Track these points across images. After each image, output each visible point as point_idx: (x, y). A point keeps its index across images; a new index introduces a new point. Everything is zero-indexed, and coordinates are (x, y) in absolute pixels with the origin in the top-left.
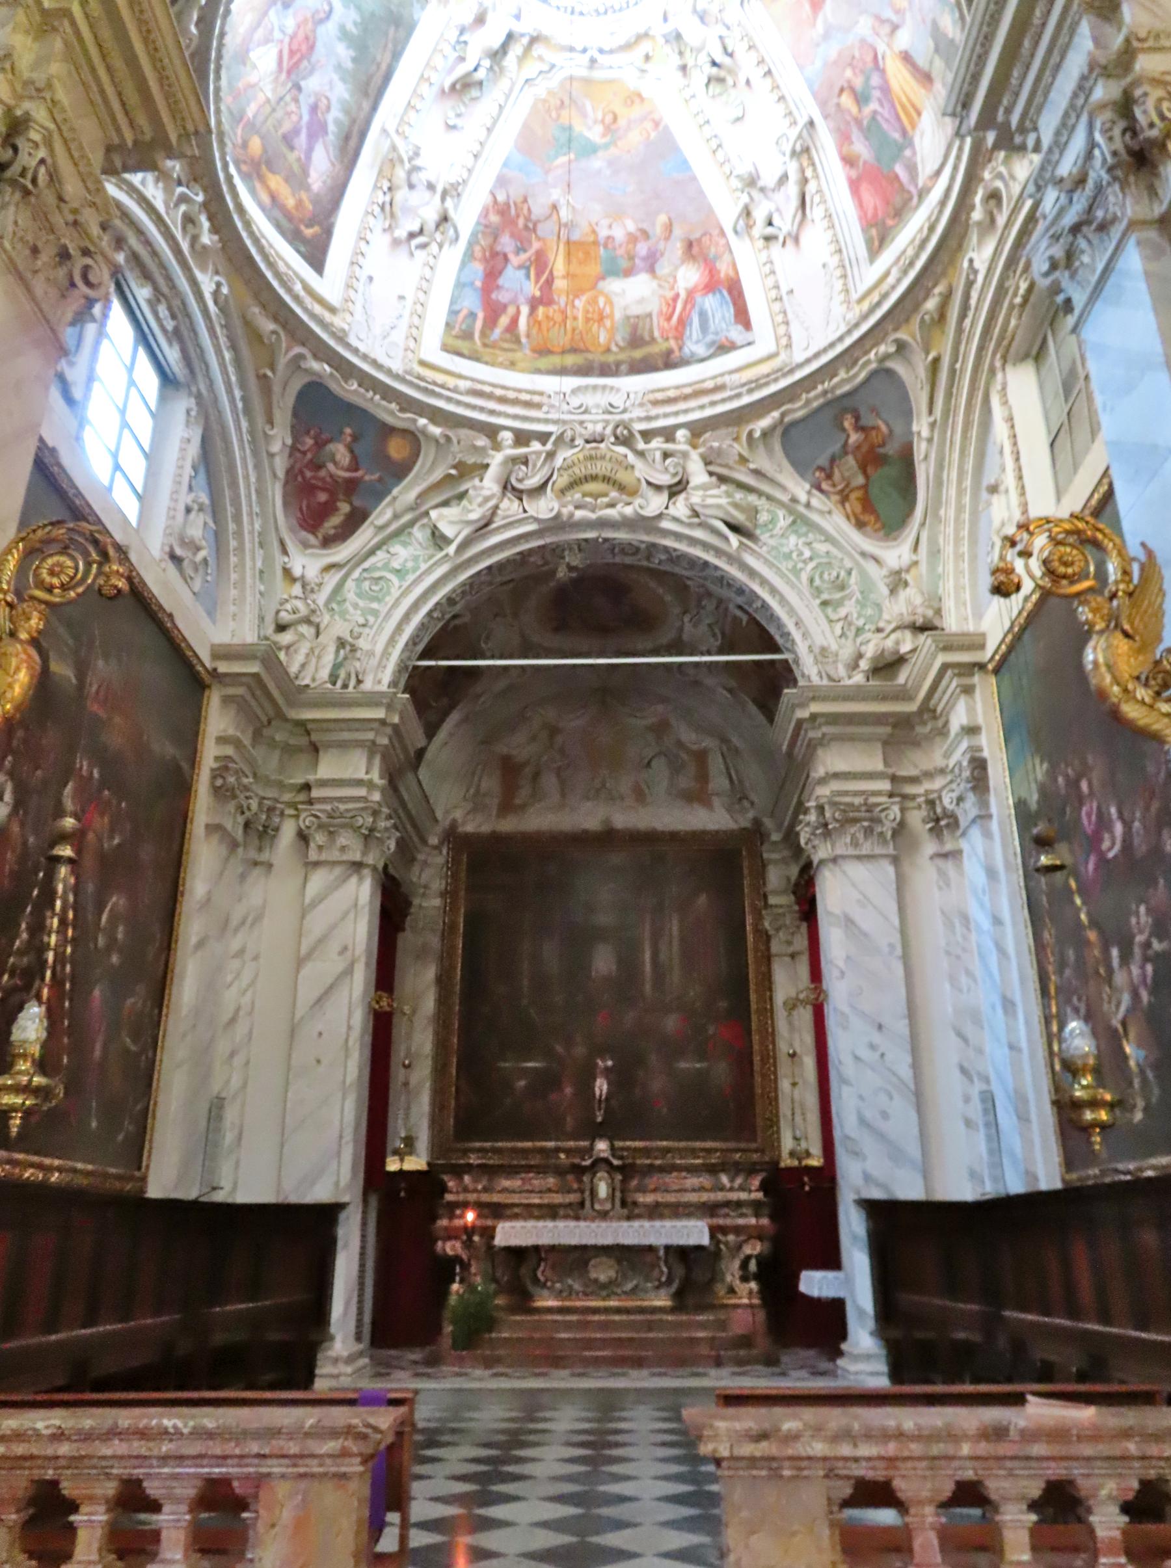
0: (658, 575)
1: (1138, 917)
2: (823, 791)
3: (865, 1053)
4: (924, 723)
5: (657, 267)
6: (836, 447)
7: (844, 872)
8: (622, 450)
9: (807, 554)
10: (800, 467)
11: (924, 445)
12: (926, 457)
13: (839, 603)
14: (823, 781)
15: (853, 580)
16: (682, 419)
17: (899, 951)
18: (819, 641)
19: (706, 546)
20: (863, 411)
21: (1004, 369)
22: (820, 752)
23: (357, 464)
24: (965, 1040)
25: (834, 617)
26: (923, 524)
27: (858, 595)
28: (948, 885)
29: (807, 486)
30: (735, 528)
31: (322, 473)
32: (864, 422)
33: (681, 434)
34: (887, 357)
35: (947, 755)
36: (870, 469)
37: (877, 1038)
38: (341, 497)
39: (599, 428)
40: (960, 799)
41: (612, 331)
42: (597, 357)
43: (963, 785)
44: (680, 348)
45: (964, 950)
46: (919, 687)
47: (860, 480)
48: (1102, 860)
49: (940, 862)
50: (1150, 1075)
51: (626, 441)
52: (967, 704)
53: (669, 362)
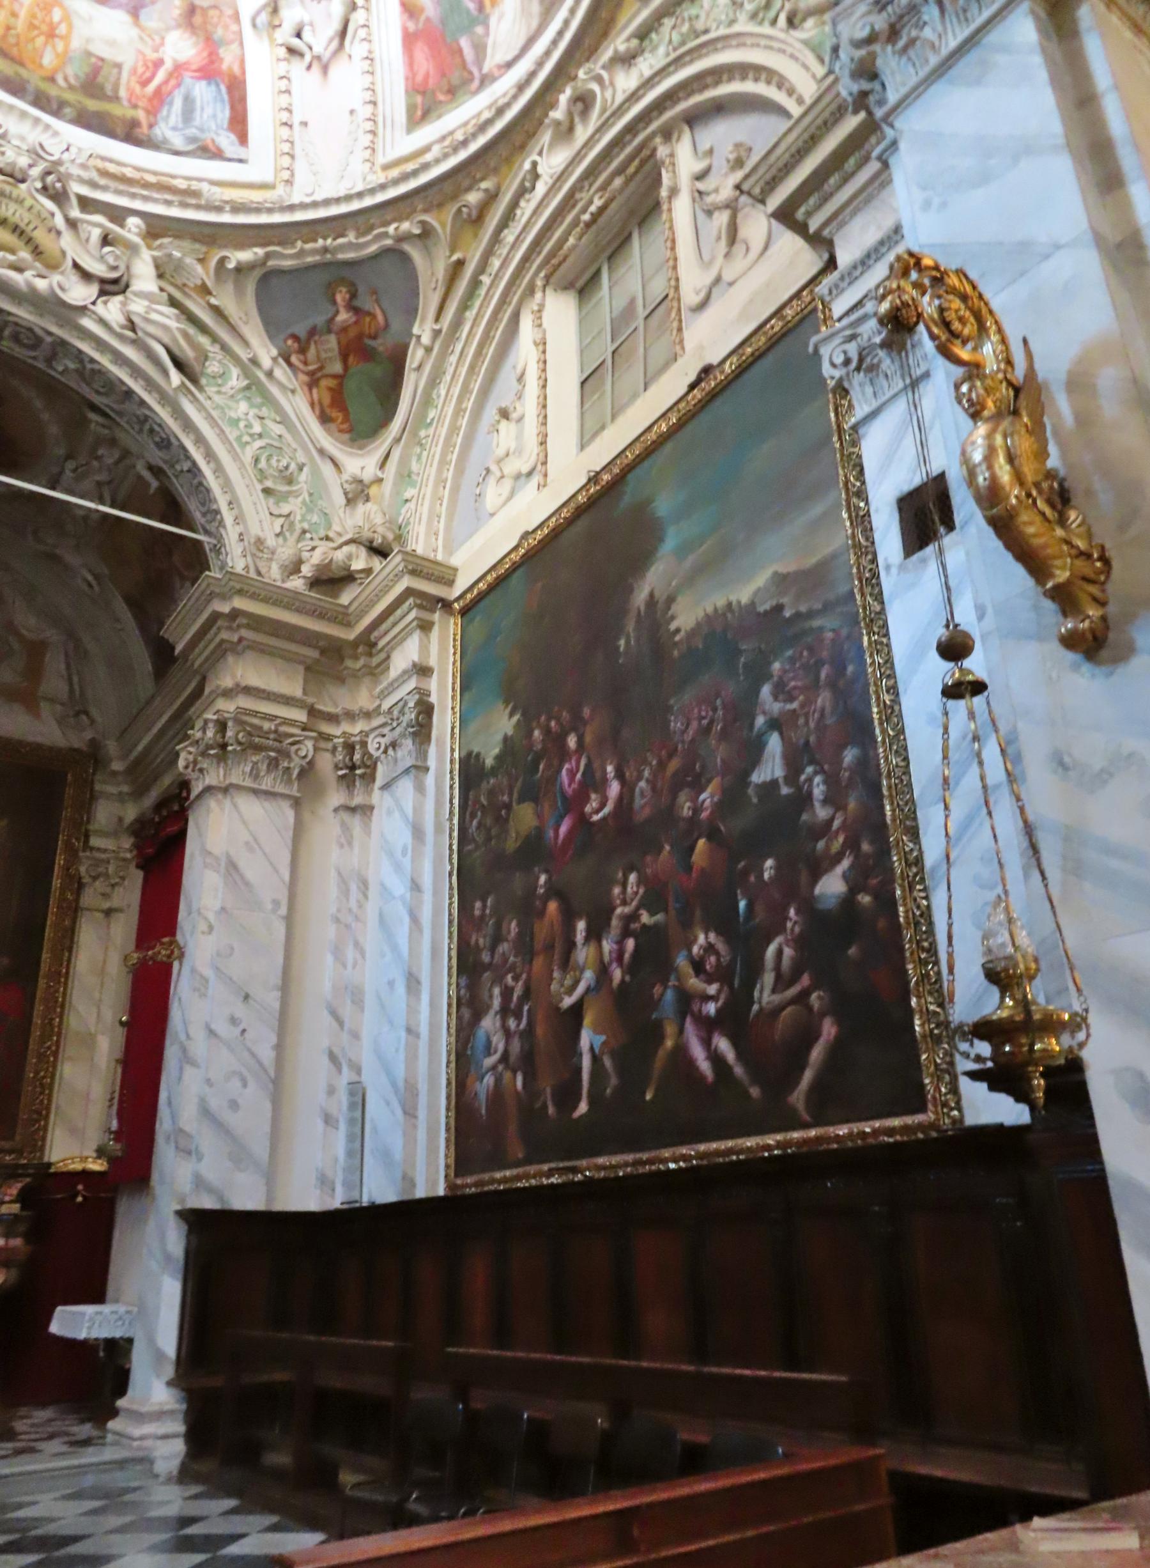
0: (52, 389)
1: (624, 885)
2: (227, 706)
3: (223, 1028)
4: (356, 658)
5: (143, 14)
6: (320, 320)
7: (235, 806)
8: (50, 205)
9: (257, 428)
10: (271, 327)
11: (420, 353)
12: (419, 368)
13: (284, 497)
14: (228, 694)
15: (303, 477)
16: (137, 205)
17: (283, 910)
18: (255, 530)
19: (136, 372)
20: (362, 289)
21: (544, 291)
22: (230, 659)
24: (341, 1023)
25: (276, 512)
26: (398, 440)
27: (306, 495)
28: (350, 843)
29: (274, 352)
30: (179, 364)
32: (357, 303)
33: (133, 222)
34: (402, 238)
35: (383, 695)
36: (351, 359)
37: (240, 1011)
39: (23, 161)
40: (394, 745)
41: (65, 58)
42: (35, 81)
43: (398, 730)
44: (151, 126)
45: (357, 919)
46: (363, 613)
47: (337, 367)
48: (582, 820)
49: (345, 816)
50: (607, 1062)
51: (59, 197)
52: (421, 640)
53: (131, 134)
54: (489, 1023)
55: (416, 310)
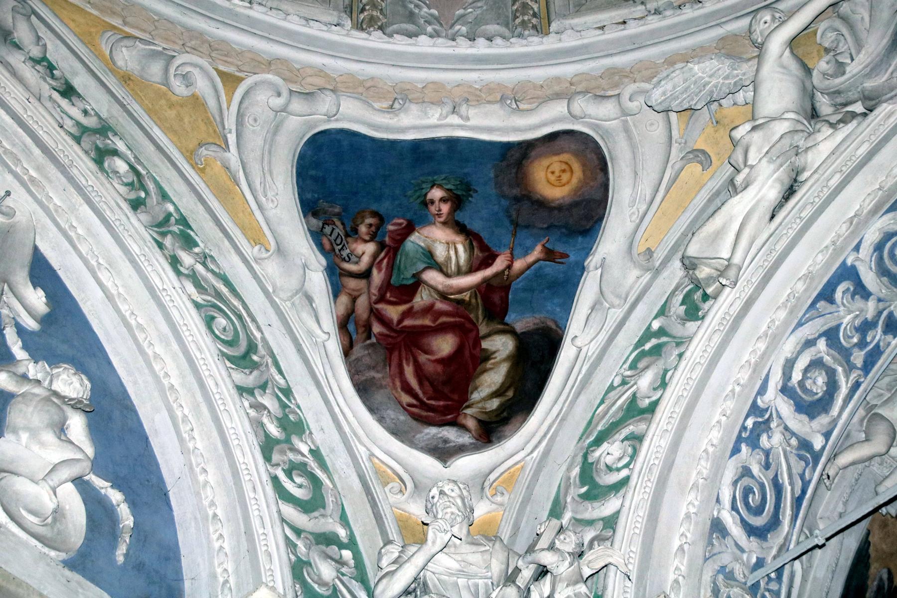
23: (484, 247)
31: (422, 298)
38: (483, 329)
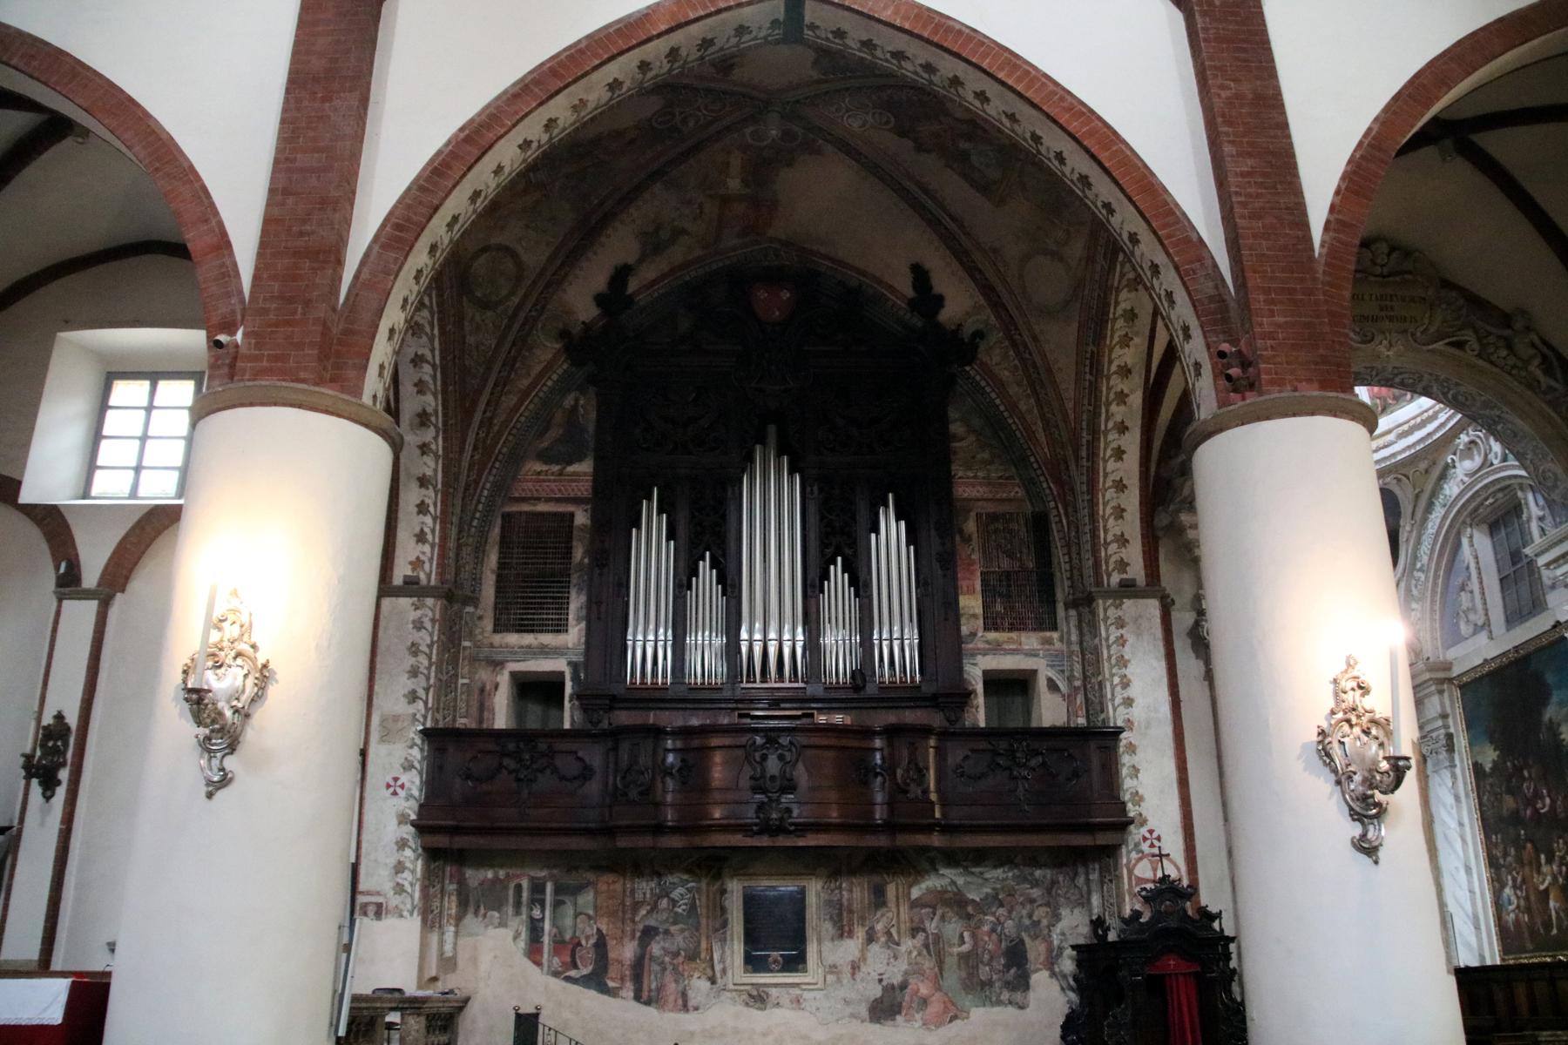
48: (1536, 811)
50: (1562, 914)
54: (1508, 891)
55: (1400, 512)
